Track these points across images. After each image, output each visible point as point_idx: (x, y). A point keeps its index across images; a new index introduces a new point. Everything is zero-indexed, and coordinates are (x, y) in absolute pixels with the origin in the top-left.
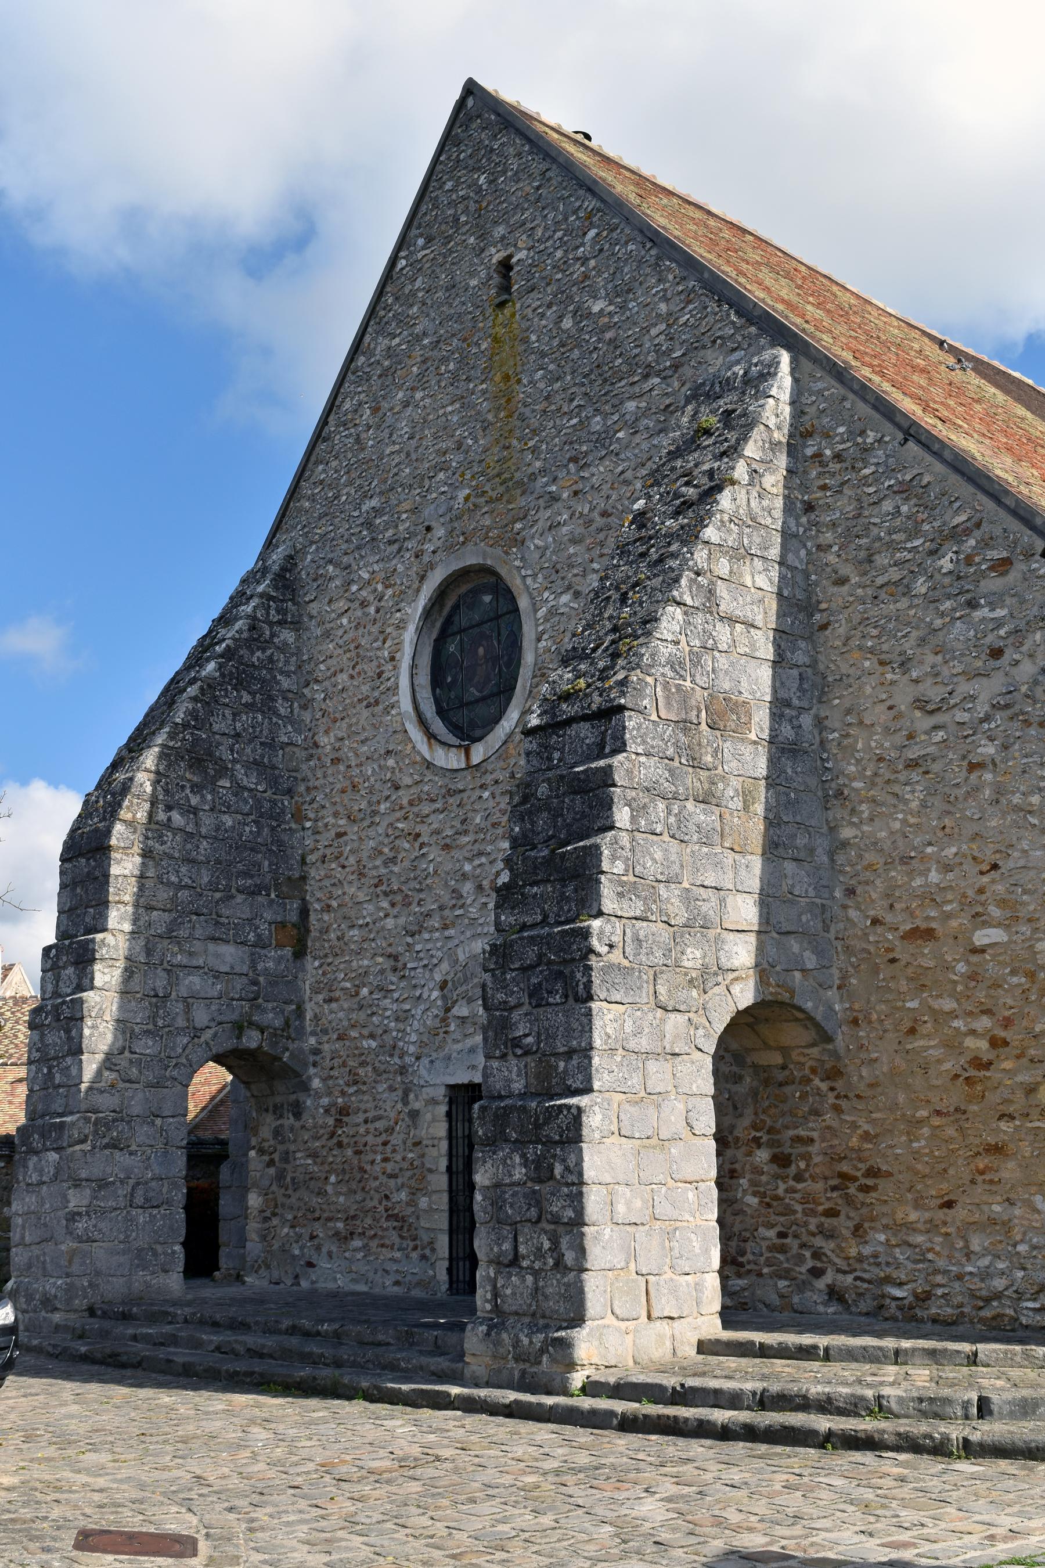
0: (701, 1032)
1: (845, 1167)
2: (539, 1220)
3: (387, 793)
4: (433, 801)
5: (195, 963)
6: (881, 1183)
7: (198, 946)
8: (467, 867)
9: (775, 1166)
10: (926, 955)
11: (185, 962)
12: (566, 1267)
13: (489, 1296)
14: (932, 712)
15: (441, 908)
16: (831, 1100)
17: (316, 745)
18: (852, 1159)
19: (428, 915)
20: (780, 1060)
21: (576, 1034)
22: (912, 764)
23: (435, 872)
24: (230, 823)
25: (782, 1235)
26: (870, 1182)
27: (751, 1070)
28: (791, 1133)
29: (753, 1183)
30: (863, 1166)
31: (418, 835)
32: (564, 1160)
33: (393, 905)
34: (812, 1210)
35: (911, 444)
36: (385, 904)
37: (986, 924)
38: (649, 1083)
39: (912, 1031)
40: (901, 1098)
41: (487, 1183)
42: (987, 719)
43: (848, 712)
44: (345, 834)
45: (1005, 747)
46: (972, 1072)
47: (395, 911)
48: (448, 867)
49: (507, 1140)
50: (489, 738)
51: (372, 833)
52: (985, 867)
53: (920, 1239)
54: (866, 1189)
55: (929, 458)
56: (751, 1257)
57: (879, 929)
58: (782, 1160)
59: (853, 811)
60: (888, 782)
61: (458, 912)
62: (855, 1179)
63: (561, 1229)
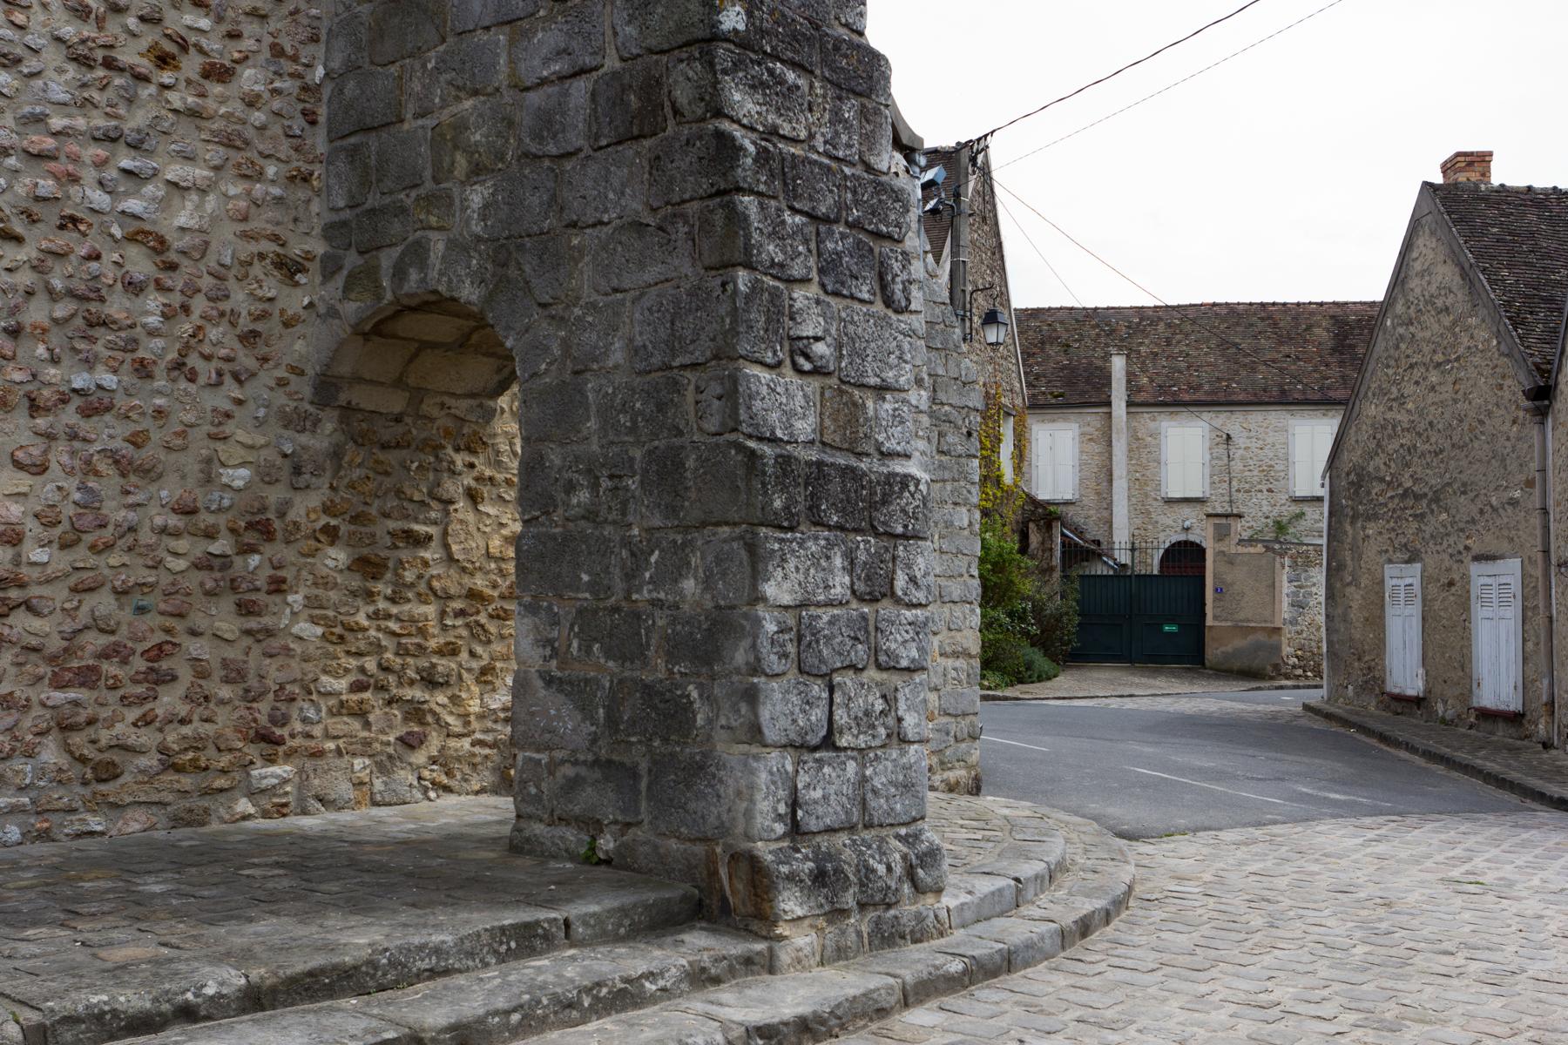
9: (357, 576)
12: (904, 741)
13: (782, 809)
18: (488, 573)
21: (893, 359)
25: (357, 687)
27: (336, 413)
28: (392, 525)
29: (312, 602)
32: (909, 566)
34: (419, 646)
41: (786, 599)
49: (818, 524)
56: (298, 727)
58: (368, 567)
62: (490, 600)
63: (896, 679)
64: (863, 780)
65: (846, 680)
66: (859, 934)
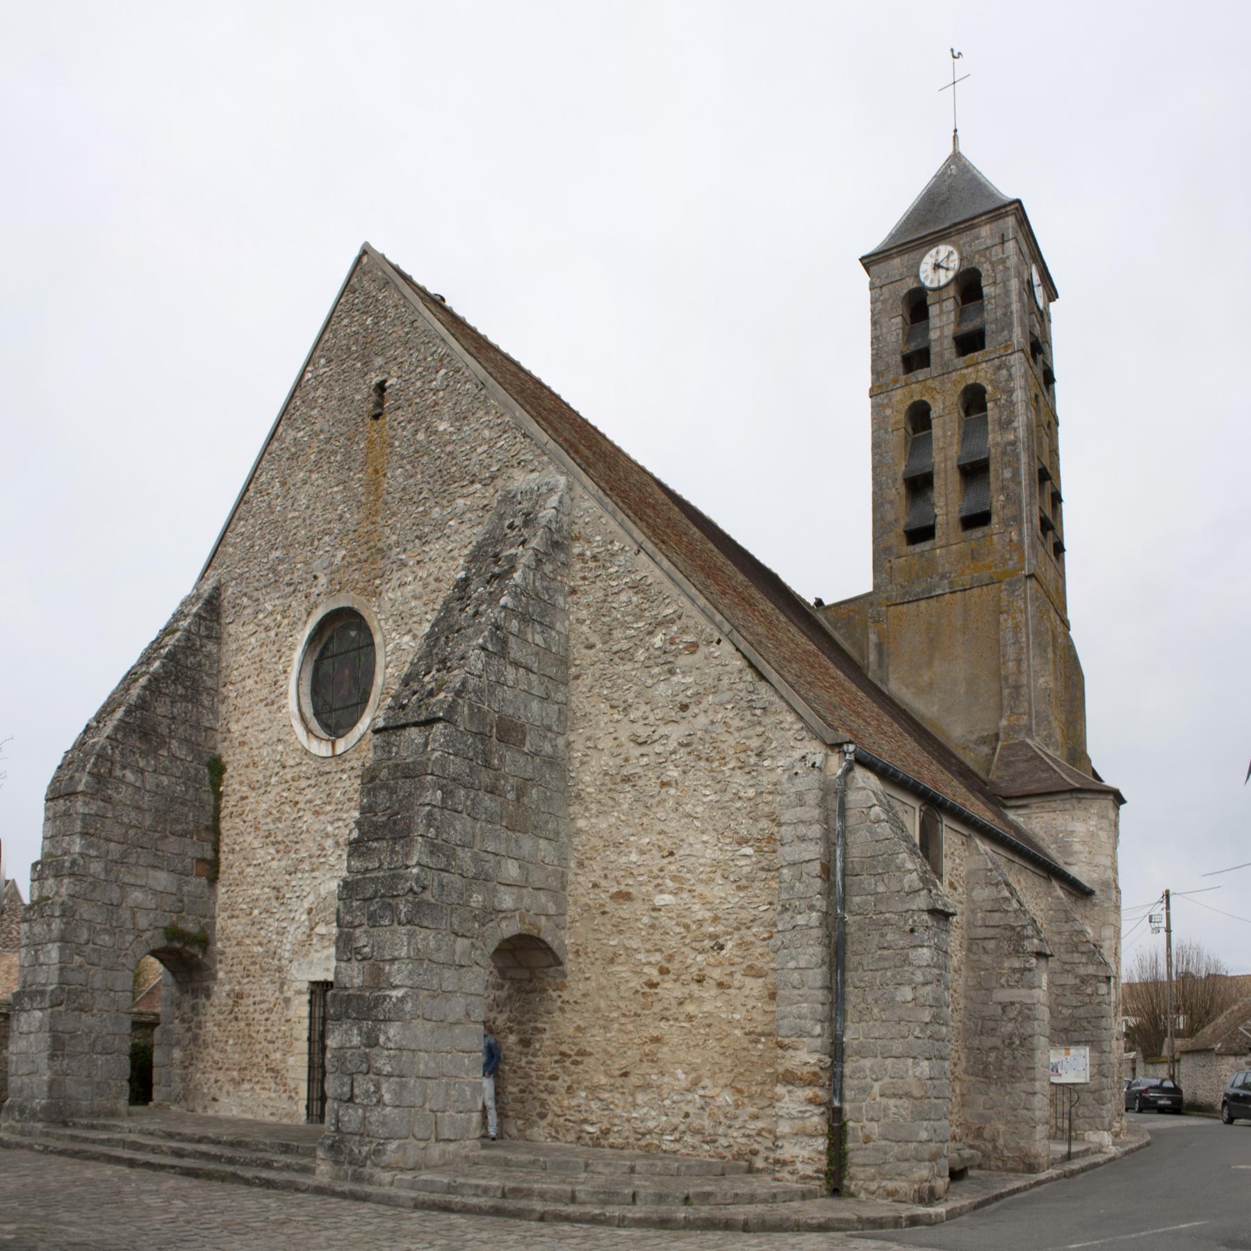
0: (479, 952)
1: (564, 1048)
2: (367, 1073)
3: (276, 770)
4: (308, 778)
5: (139, 883)
6: (586, 1060)
7: (142, 871)
8: (330, 828)
10: (625, 910)
11: (132, 881)
12: (385, 1105)
14: (640, 744)
15: (311, 857)
16: (559, 1003)
17: (229, 731)
19: (302, 861)
20: (528, 976)
22: (626, 779)
23: (308, 831)
24: (166, 783)
26: (579, 1059)
30: (576, 1048)
31: (297, 803)
33: (278, 852)
35: (642, 554)
36: (272, 851)
37: (662, 892)
38: (444, 985)
39: (612, 961)
40: (603, 1004)
42: (674, 752)
43: (589, 739)
44: (246, 798)
45: (684, 772)
46: (647, 989)
47: (279, 856)
48: (316, 826)
50: (349, 736)
51: (265, 798)
52: (665, 854)
53: (606, 1095)
54: (576, 1063)
55: (652, 565)
57: (597, 891)
59: (587, 809)
60: (610, 790)
61: (322, 860)
63: (382, 1079)
64: (365, 1118)
65: (359, 1078)
66: (346, 1174)
